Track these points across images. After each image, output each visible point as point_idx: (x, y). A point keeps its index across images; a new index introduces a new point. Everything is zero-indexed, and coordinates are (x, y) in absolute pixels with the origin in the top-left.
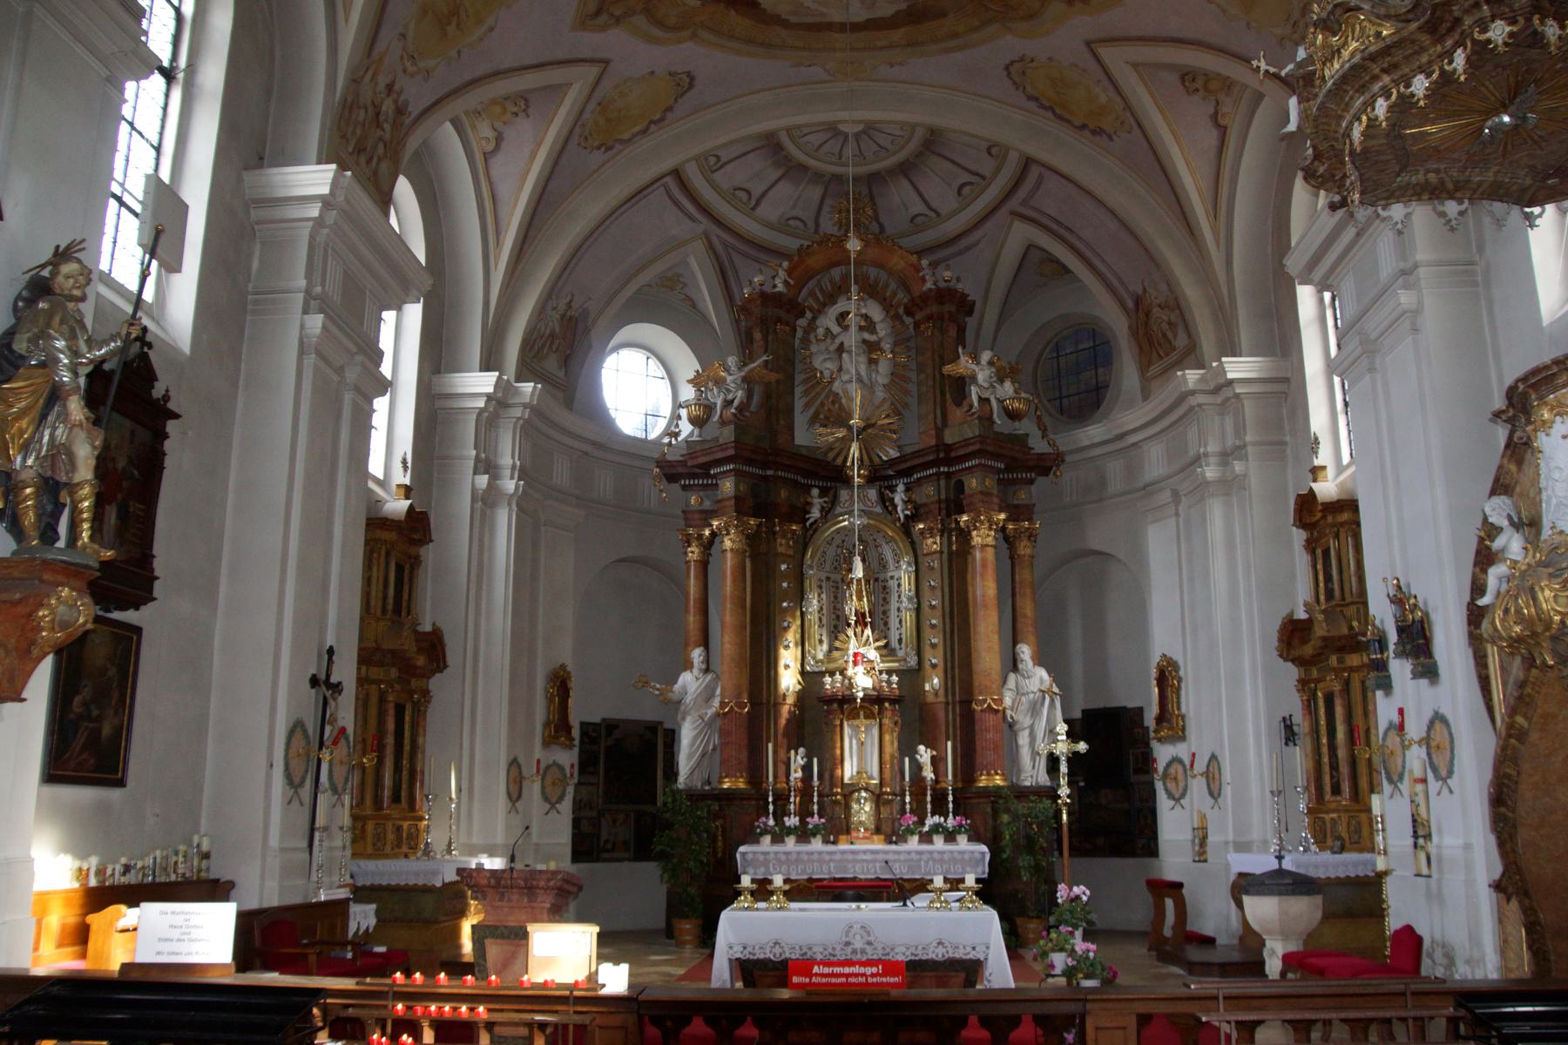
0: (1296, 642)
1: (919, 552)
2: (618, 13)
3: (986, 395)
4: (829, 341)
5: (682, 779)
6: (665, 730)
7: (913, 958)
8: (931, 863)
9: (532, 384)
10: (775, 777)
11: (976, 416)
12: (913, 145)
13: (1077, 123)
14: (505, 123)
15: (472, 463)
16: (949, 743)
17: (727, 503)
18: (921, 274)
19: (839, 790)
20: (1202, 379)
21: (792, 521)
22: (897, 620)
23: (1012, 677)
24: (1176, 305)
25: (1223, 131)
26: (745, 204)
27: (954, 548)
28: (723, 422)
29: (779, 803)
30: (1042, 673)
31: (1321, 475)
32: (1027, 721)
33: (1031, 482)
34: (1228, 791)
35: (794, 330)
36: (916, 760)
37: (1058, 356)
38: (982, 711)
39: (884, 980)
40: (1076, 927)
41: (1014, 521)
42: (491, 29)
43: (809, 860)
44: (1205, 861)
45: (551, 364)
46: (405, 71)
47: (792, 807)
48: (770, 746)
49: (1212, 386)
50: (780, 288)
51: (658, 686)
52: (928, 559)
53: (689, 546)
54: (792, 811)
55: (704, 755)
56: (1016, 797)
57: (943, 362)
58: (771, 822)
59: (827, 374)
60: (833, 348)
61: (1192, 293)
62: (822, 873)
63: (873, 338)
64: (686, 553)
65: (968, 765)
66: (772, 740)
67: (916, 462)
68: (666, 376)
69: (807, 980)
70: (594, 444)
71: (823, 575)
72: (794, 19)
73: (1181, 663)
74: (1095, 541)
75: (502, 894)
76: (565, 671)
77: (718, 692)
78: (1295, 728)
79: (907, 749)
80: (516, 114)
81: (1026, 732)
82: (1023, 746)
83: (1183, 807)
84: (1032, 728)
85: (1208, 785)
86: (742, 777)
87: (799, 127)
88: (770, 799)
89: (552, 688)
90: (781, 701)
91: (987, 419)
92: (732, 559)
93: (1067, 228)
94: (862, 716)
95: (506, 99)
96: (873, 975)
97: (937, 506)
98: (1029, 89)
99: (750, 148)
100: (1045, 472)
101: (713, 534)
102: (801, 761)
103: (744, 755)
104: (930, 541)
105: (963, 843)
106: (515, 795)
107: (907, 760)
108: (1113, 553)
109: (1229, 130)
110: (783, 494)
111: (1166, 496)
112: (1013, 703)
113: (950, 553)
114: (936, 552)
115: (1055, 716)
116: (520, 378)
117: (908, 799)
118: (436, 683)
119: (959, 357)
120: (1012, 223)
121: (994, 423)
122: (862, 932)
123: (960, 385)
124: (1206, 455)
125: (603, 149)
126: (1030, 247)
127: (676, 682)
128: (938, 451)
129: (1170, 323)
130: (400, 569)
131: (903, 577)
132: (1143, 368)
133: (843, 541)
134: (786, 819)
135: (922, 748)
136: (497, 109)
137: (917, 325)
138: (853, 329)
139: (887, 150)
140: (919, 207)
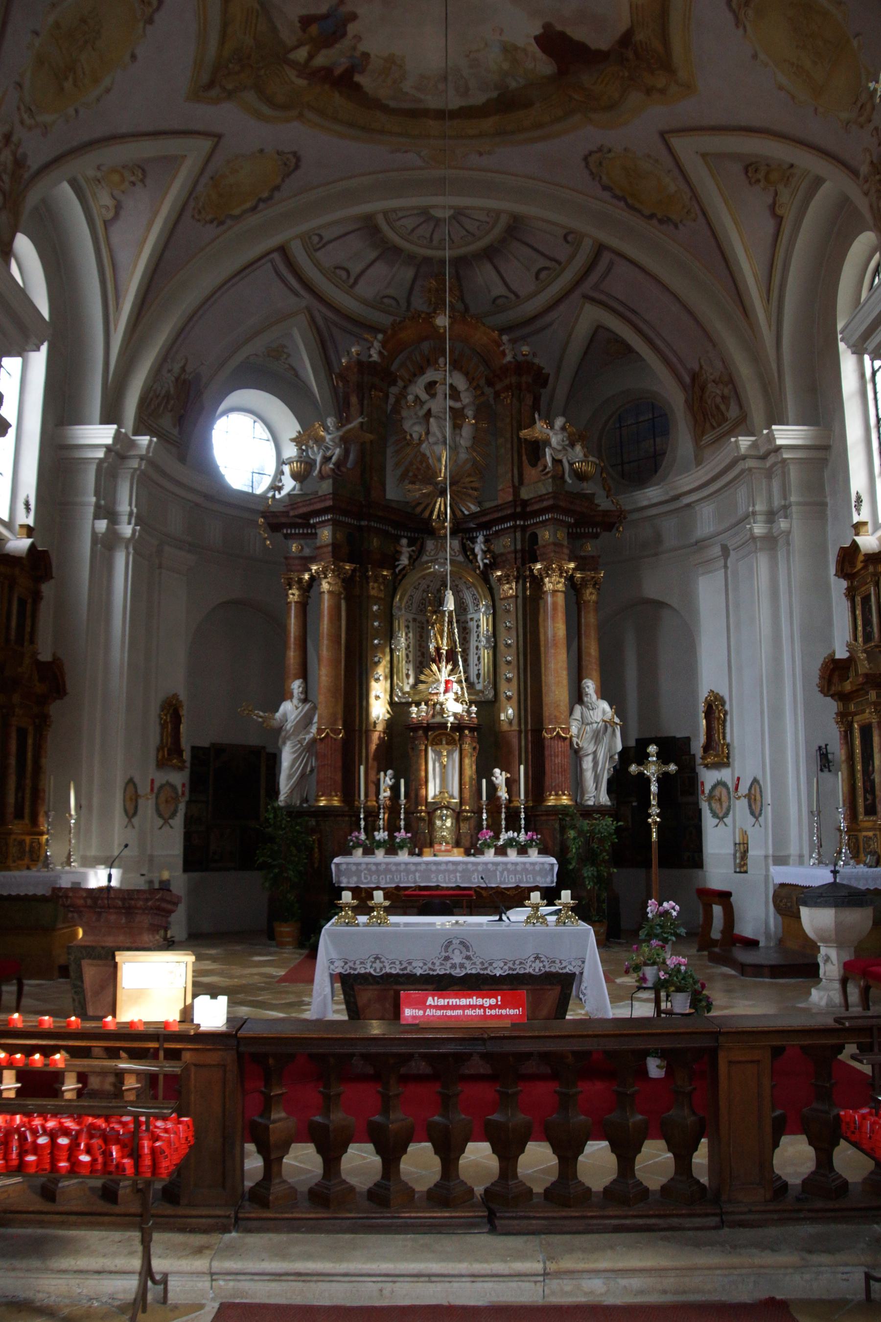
0: (835, 679)
1: (496, 598)
2: (230, 87)
3: (559, 457)
4: (418, 408)
5: (282, 797)
6: (268, 754)
7: (511, 972)
8: (505, 873)
9: (148, 438)
10: (366, 795)
11: (550, 475)
12: (498, 231)
13: (647, 212)
14: (123, 192)
15: (91, 510)
16: (522, 767)
17: (325, 550)
18: (501, 349)
19: (423, 808)
20: (754, 445)
21: (383, 568)
22: (476, 657)
23: (578, 709)
24: (729, 380)
25: (779, 220)
26: (343, 281)
27: (528, 593)
28: (322, 477)
29: (370, 819)
30: (604, 705)
31: (863, 530)
32: (591, 748)
33: (596, 536)
34: (769, 811)
35: (387, 396)
36: (492, 781)
37: (620, 427)
38: (551, 738)
39: (504, 1012)
40: (666, 941)
41: (580, 570)
42: (108, 91)
43: (397, 871)
44: (746, 872)
45: (166, 422)
46: (22, 122)
47: (381, 822)
48: (362, 768)
49: (762, 451)
50: (375, 357)
51: (261, 714)
52: (505, 603)
53: (290, 589)
54: (382, 826)
55: (303, 776)
56: (581, 815)
57: (520, 428)
58: (363, 837)
59: (415, 436)
60: (422, 413)
61: (744, 370)
62: (408, 882)
63: (458, 405)
64: (287, 595)
65: (537, 789)
66: (364, 762)
67: (496, 515)
68: (270, 438)
69: (421, 1013)
70: (207, 497)
71: (410, 617)
72: (392, 104)
73: (727, 698)
74: (652, 589)
75: (100, 914)
76: (177, 699)
77: (316, 719)
78: (830, 756)
79: (484, 771)
80: (133, 184)
81: (590, 758)
82: (587, 770)
83: (726, 825)
84: (595, 753)
85: (750, 806)
86: (336, 796)
87: (395, 210)
88: (362, 816)
89: (166, 715)
90: (372, 728)
91: (559, 478)
92: (329, 600)
93: (633, 311)
94: (444, 742)
95: (124, 167)
96: (491, 1007)
97: (513, 555)
98: (604, 178)
99: (350, 229)
100: (609, 527)
101: (312, 578)
102: (389, 782)
103: (339, 777)
104: (506, 587)
105: (534, 855)
106: (131, 812)
107: (484, 781)
108: (667, 600)
109: (784, 220)
110: (375, 542)
111: (717, 551)
112: (578, 732)
113: (525, 597)
114: (511, 597)
115: (615, 743)
116: (136, 433)
117: (484, 816)
118: (54, 708)
119: (535, 423)
120: (582, 308)
121: (565, 482)
122: (461, 947)
123: (536, 449)
124: (754, 513)
125: (215, 223)
126: (599, 328)
127: (277, 710)
128: (515, 507)
129: (723, 397)
130: (22, 603)
131: (483, 621)
132: (698, 437)
133: (428, 586)
134: (376, 833)
135: (497, 771)
136: (116, 178)
137: (497, 394)
138: (440, 396)
139: (474, 235)
140: (501, 291)
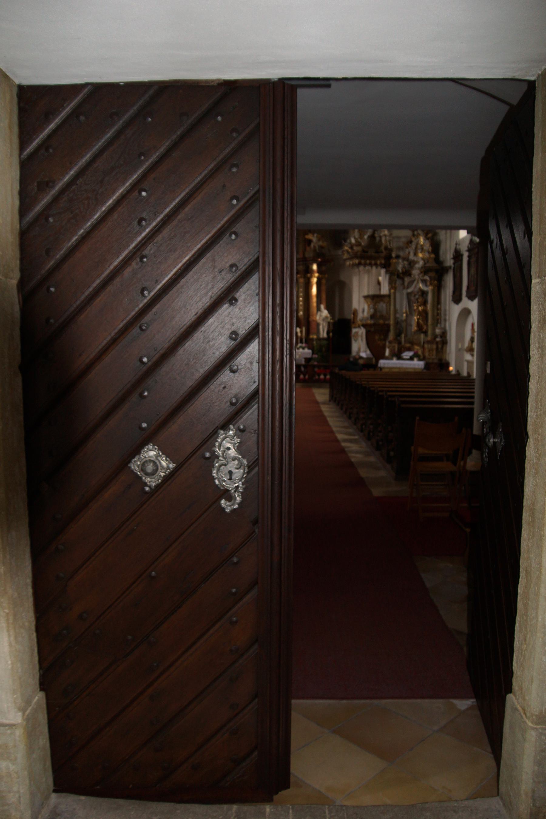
65: (308, 332)
105: (306, 350)
